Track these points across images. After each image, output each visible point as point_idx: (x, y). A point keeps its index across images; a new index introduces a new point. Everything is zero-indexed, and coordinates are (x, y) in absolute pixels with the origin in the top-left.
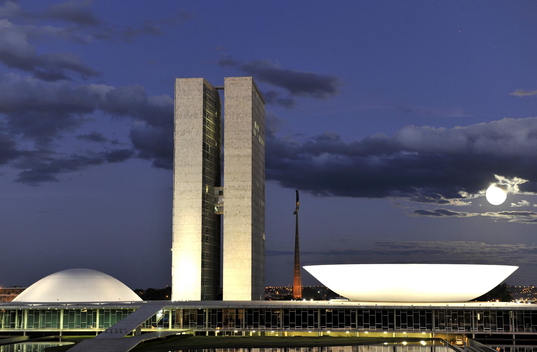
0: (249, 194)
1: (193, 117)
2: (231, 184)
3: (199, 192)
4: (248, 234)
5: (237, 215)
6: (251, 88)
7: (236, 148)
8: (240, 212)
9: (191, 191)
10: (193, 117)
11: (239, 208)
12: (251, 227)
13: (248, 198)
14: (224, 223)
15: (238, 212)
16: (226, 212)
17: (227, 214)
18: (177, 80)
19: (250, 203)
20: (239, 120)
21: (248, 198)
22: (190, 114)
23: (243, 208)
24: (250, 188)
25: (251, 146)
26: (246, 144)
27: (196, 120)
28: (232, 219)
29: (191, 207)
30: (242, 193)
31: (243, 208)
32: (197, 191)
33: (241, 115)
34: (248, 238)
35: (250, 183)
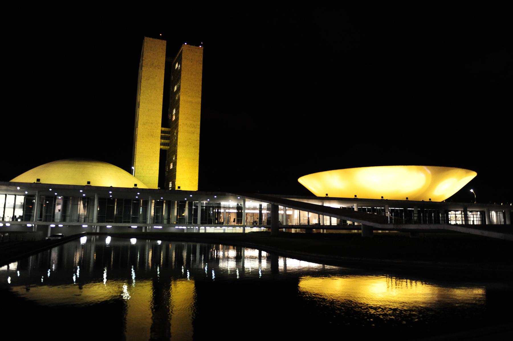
0: (198, 131)
1: (157, 68)
5: (188, 145)
7: (189, 96)
9: (152, 123)
10: (157, 68)
12: (198, 156)
18: (146, 38)
19: (199, 138)
20: (193, 77)
22: (154, 65)
24: (199, 127)
25: (200, 96)
26: (197, 95)
27: (159, 70)
29: (152, 135)
30: (193, 129)
33: (194, 73)
35: (199, 123)
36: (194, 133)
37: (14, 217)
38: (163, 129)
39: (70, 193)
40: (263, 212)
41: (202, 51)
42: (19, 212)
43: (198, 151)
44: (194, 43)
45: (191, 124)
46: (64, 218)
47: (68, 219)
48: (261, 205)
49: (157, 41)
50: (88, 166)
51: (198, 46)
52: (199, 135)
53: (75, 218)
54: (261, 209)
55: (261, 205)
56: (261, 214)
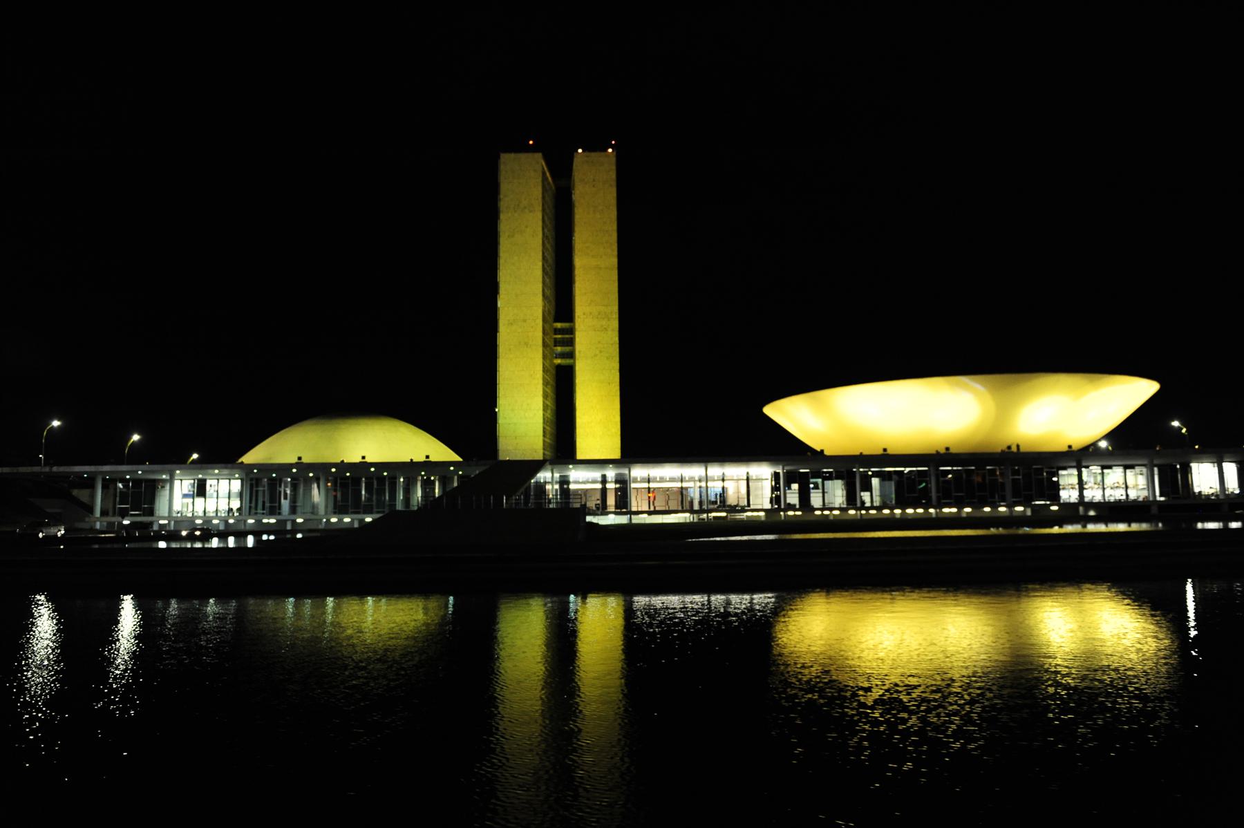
0: (615, 324)
6: (614, 167)
9: (525, 321)
20: (598, 216)
24: (616, 316)
25: (616, 253)
29: (526, 344)
30: (604, 323)
35: (616, 308)
37: (230, 510)
38: (559, 325)
39: (304, 473)
40: (608, 486)
41: (613, 160)
42: (236, 504)
43: (617, 366)
44: (596, 146)
46: (293, 510)
47: (299, 510)
48: (604, 477)
49: (523, 157)
50: (343, 426)
51: (606, 150)
52: (617, 333)
53: (309, 509)
54: (604, 480)
55: (604, 477)
56: (604, 491)
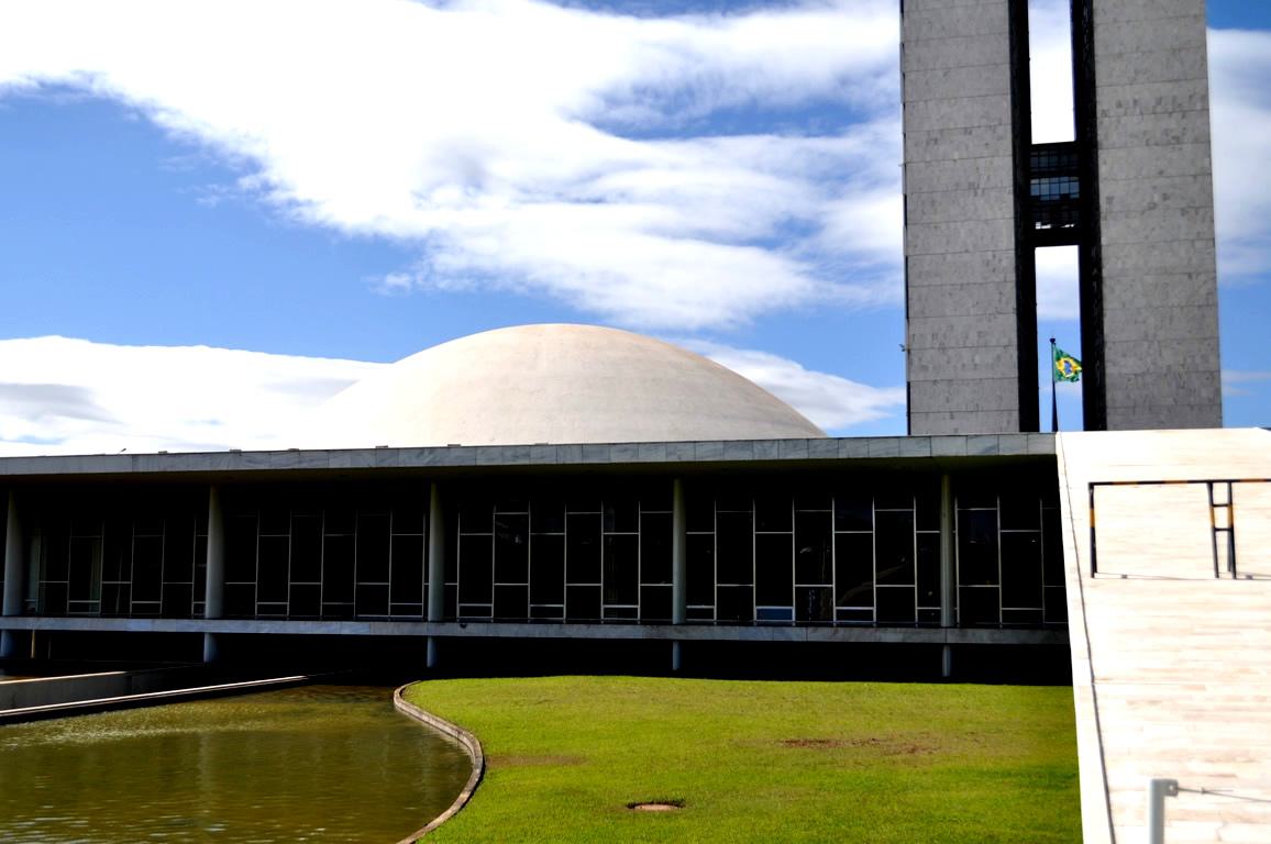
2: (1127, 94)
3: (1000, 130)
4: (1203, 278)
5: (1153, 206)
8: (1165, 197)
9: (967, 131)
11: (1161, 181)
13: (1196, 141)
14: (1104, 241)
15: (1157, 198)
16: (1110, 200)
17: (1116, 207)
21: (1196, 141)
23: (1177, 180)
28: (1136, 223)
29: (973, 188)
30: (1172, 123)
31: (1177, 180)
32: (993, 129)
34: (1203, 291)
36: (1178, 140)
45: (1159, 101)
